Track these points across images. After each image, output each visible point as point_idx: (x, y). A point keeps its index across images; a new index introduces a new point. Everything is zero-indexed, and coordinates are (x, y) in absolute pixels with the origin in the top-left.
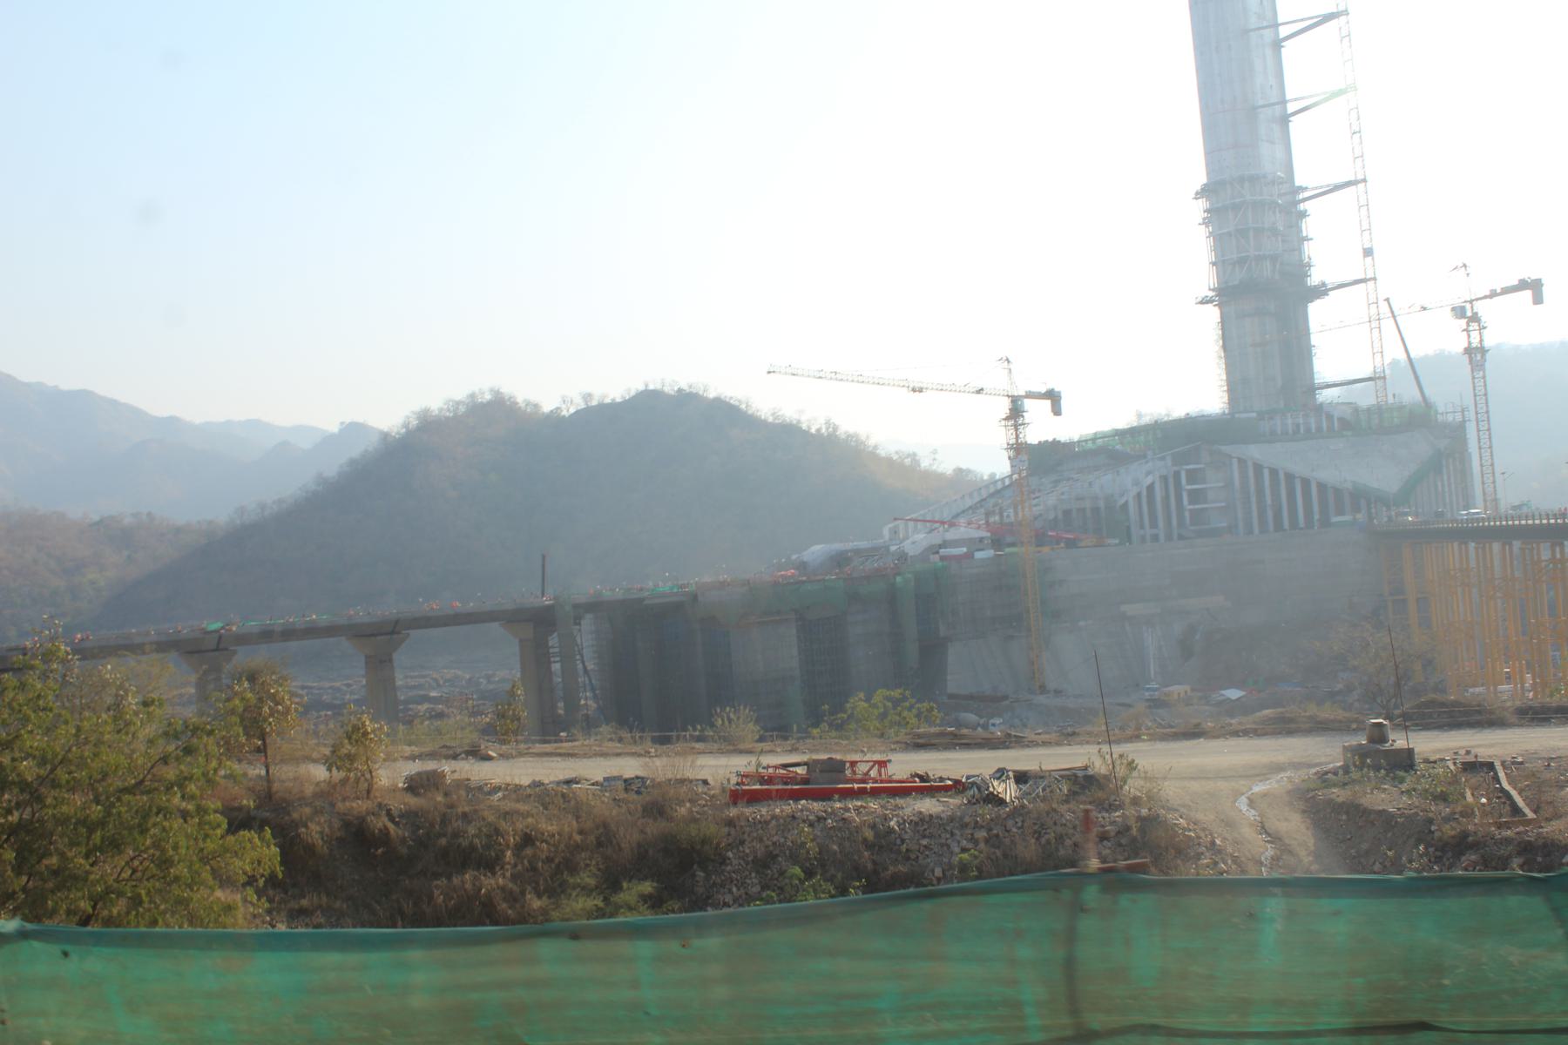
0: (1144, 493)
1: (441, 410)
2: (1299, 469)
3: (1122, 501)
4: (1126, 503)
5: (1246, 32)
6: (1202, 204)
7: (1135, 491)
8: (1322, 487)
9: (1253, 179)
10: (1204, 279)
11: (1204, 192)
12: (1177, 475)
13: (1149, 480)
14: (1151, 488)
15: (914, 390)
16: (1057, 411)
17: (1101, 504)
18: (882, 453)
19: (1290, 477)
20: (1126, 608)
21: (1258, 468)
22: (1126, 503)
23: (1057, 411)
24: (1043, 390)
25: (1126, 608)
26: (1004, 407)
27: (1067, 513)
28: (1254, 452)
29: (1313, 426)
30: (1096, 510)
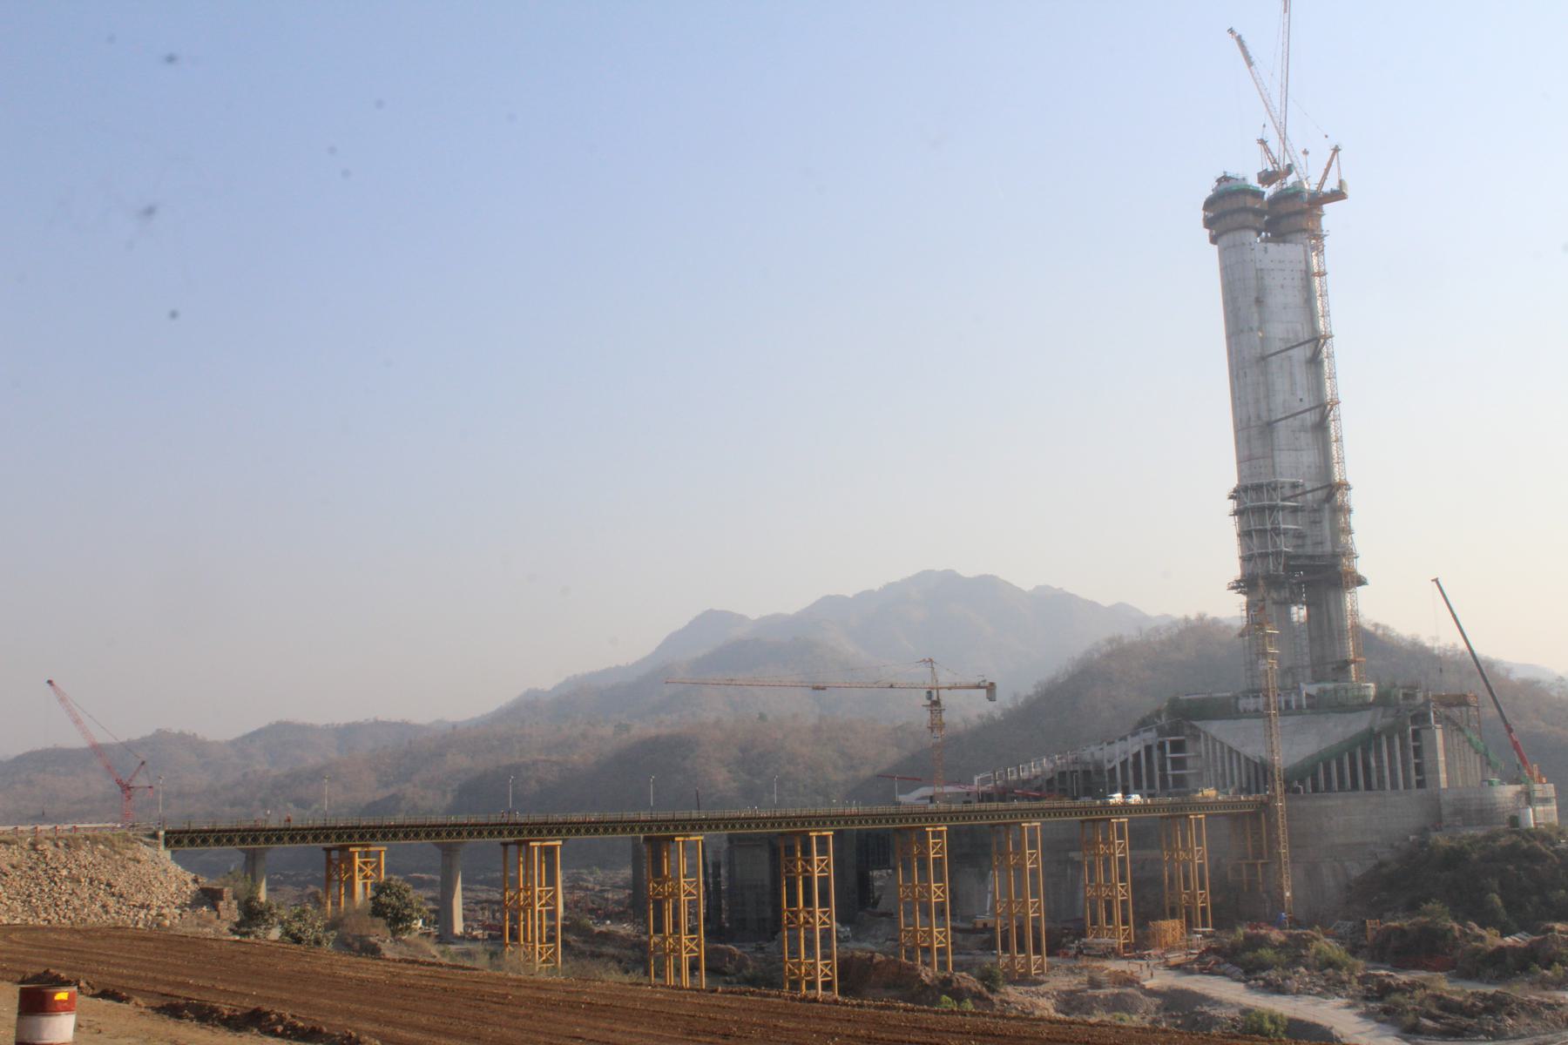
0: (1131, 759)
1: (1355, 614)
2: (1235, 745)
3: (1108, 766)
4: (1114, 769)
5: (1263, 358)
6: (1232, 505)
7: (1123, 758)
8: (1247, 759)
9: (1258, 488)
10: (1235, 571)
11: (1236, 495)
12: (1162, 746)
13: (1136, 749)
14: (1137, 755)
15: (818, 688)
16: (991, 698)
17: (1091, 768)
18: (1514, 677)
19: (1231, 750)
20: (1072, 854)
21: (1214, 739)
22: (1114, 769)
23: (991, 698)
24: (976, 681)
25: (1072, 854)
26: (924, 693)
27: (1062, 774)
28: (1215, 728)
29: (1293, 704)
30: (1087, 773)
